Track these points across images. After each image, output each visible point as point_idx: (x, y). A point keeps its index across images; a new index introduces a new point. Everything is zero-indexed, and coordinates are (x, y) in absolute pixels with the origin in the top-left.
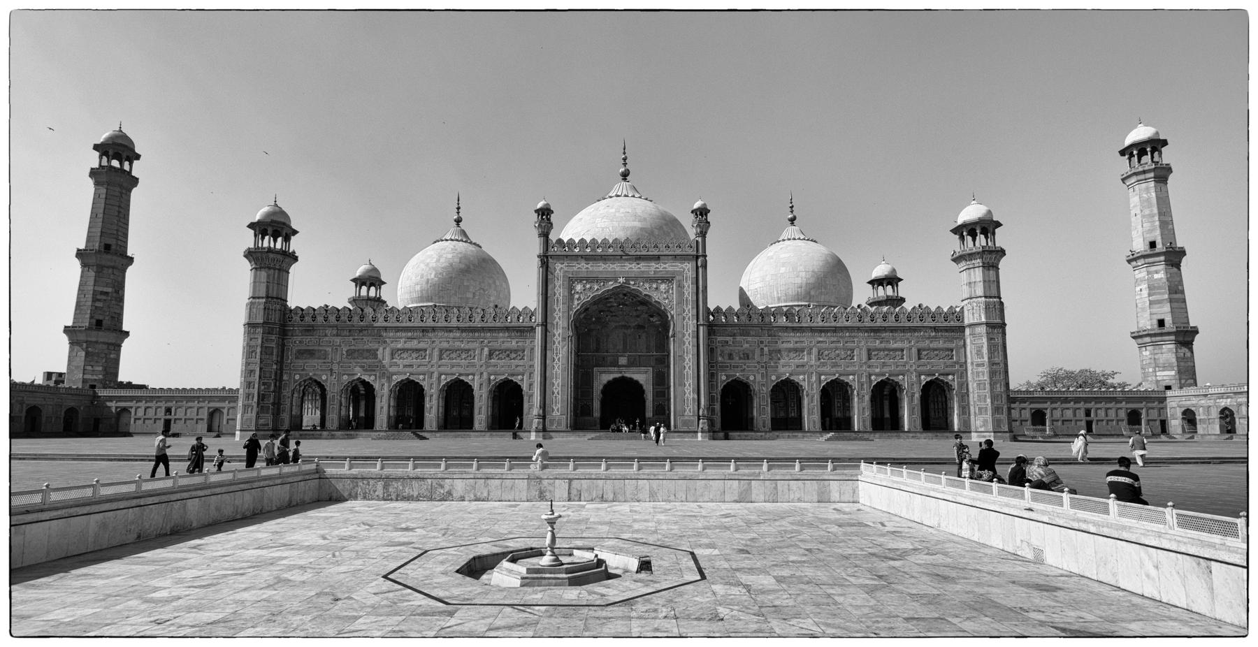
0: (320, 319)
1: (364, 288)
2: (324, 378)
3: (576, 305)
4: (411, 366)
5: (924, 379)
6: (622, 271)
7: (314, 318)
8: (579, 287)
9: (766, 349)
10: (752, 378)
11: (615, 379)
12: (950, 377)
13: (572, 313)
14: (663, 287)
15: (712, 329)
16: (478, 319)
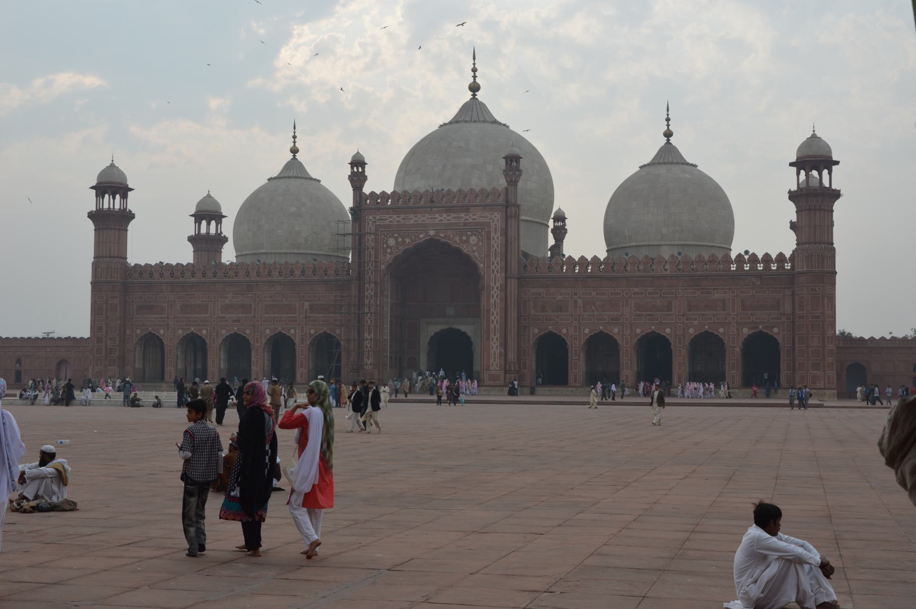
0: (156, 275)
1: (204, 223)
2: (162, 332)
3: (389, 258)
4: (238, 321)
5: (746, 331)
6: (433, 225)
7: (151, 275)
8: (392, 242)
9: (580, 301)
10: (564, 331)
11: (442, 330)
12: (776, 330)
13: (383, 267)
14: (473, 240)
15: (522, 281)
16: (297, 272)
